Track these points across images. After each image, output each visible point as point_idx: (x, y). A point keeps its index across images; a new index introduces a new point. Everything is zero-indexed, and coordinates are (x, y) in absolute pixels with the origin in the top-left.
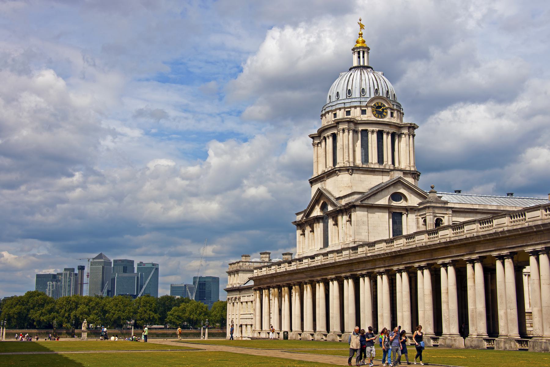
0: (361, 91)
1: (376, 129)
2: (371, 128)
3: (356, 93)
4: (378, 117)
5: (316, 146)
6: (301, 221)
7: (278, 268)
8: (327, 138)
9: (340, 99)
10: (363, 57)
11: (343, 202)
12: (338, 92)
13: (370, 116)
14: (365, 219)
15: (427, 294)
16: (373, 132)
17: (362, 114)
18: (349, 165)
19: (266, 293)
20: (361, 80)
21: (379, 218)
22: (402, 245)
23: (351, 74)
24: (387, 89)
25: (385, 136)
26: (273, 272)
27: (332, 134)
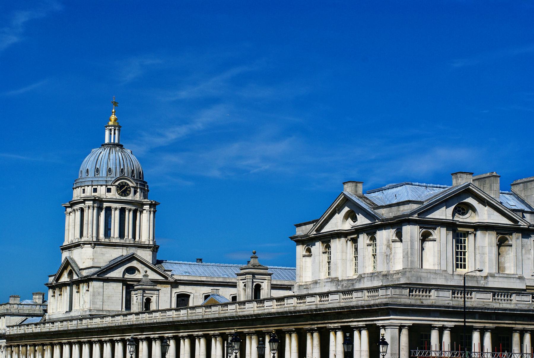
0: (108, 170)
1: (119, 206)
2: (114, 206)
3: (103, 172)
4: (122, 196)
5: (69, 215)
6: (52, 284)
7: (27, 329)
8: (76, 211)
9: (89, 176)
10: (115, 134)
11: (85, 273)
12: (88, 169)
13: (114, 194)
14: (101, 290)
15: (157, 355)
16: (116, 209)
17: (107, 192)
18: (92, 240)
19: (16, 351)
20: (109, 160)
21: (113, 289)
22: (108, 322)
23: (101, 152)
24: (132, 168)
25: (127, 213)
26: (22, 332)
27: (80, 208)
